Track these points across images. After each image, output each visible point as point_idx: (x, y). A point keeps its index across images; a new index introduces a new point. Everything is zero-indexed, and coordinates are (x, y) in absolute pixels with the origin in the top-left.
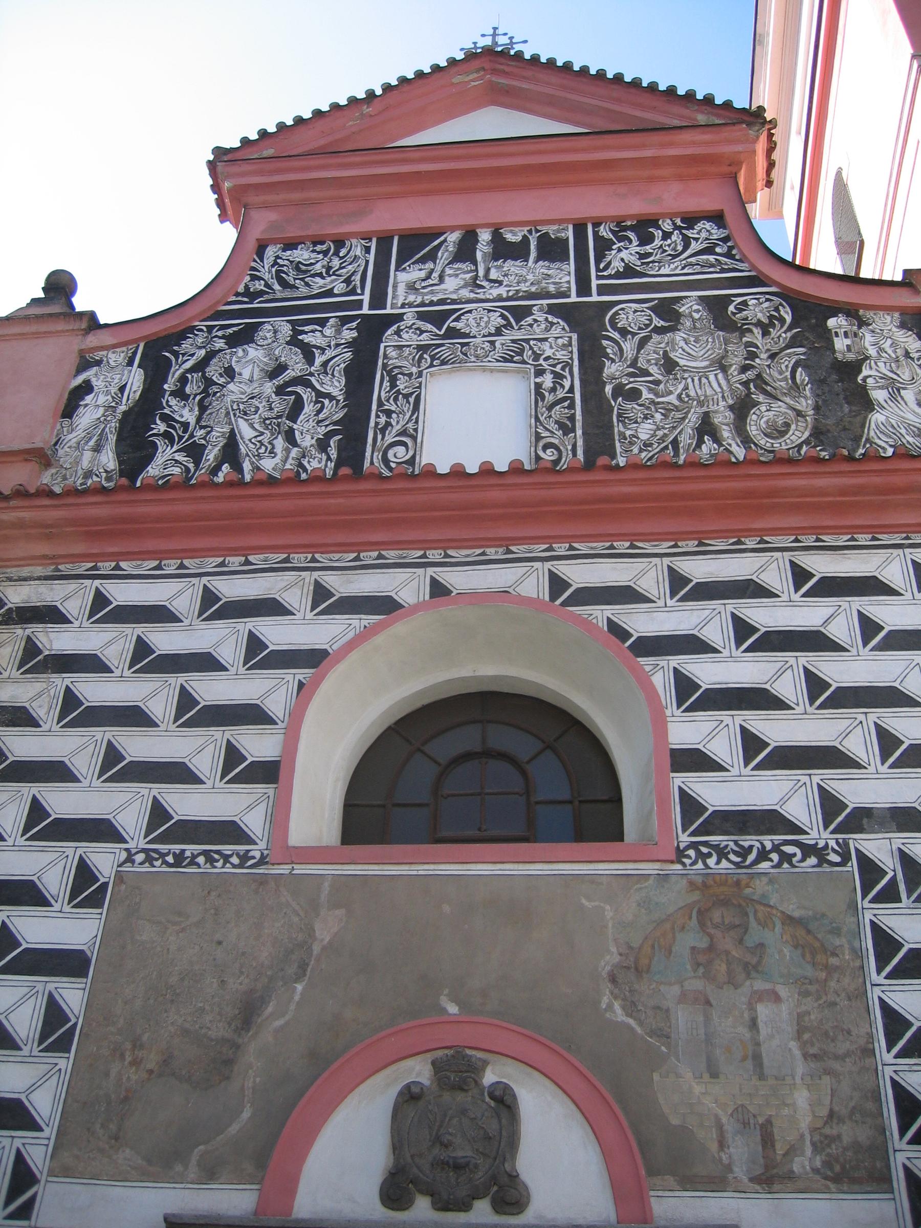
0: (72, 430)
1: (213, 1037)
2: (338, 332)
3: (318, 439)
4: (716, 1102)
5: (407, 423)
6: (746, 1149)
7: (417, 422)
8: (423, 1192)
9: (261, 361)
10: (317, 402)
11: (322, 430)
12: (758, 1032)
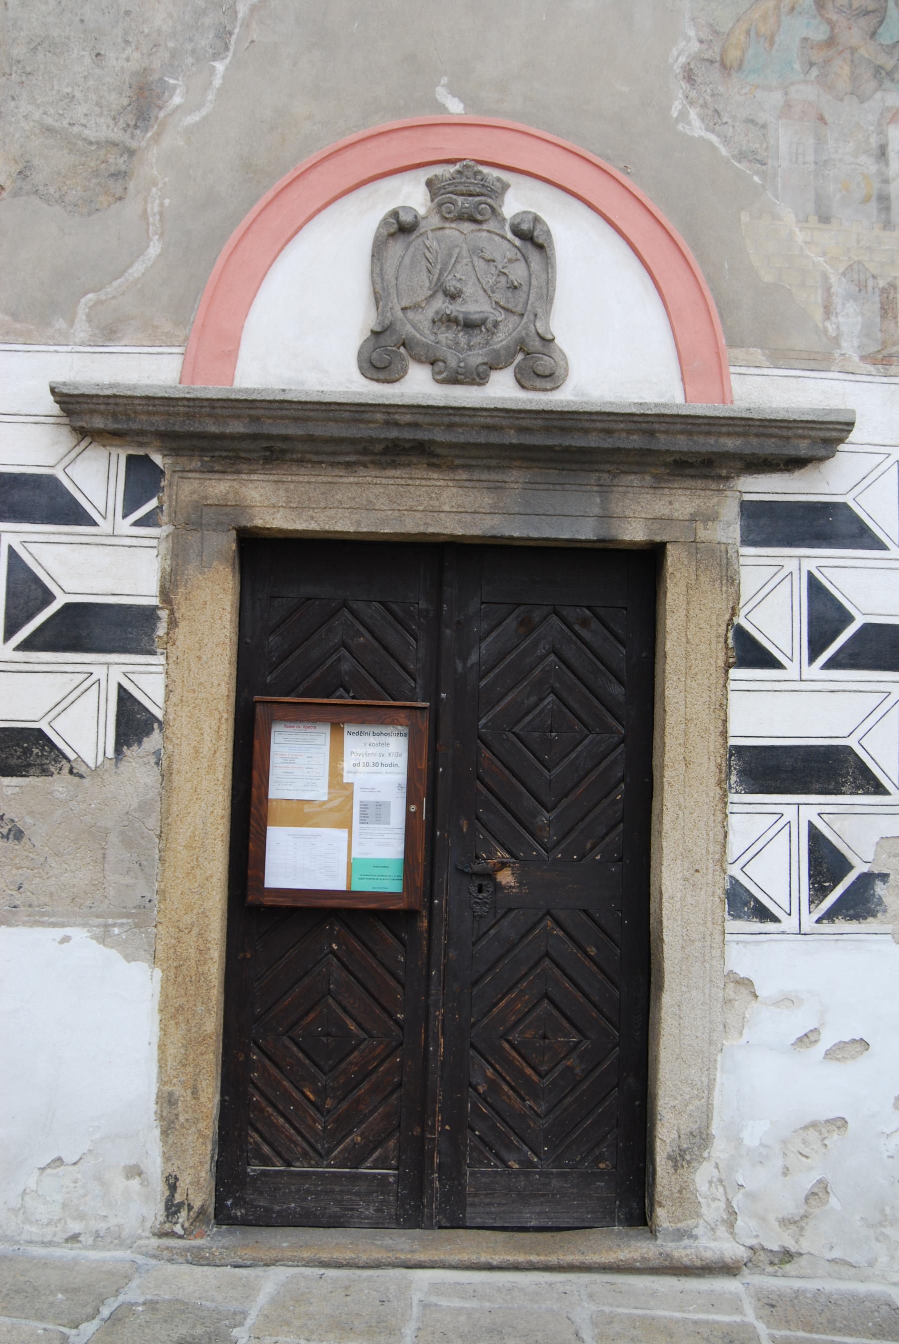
1: (93, 139)
4: (824, 254)
6: (859, 319)
8: (419, 360)
12: (887, 164)
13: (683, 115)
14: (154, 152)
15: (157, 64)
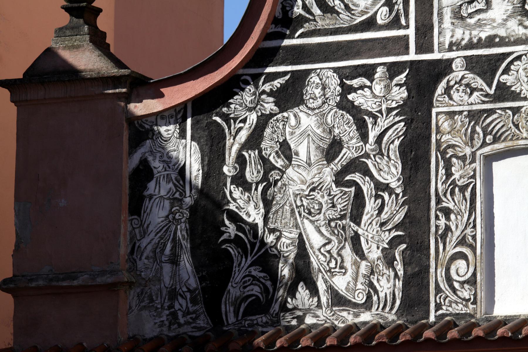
0: (145, 233)
2: (388, 88)
3: (384, 249)
5: (466, 228)
7: (474, 227)
9: (315, 133)
10: (377, 197)
11: (387, 237)
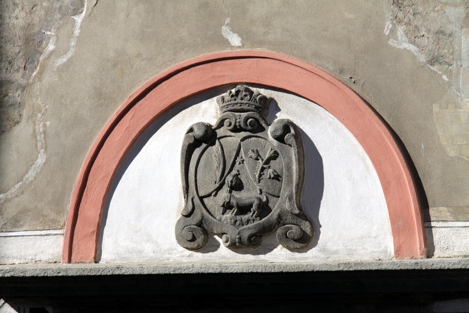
13: (393, 31)
14: (37, 86)
15: (36, 20)
